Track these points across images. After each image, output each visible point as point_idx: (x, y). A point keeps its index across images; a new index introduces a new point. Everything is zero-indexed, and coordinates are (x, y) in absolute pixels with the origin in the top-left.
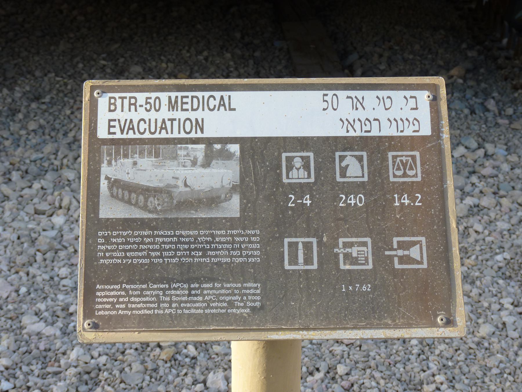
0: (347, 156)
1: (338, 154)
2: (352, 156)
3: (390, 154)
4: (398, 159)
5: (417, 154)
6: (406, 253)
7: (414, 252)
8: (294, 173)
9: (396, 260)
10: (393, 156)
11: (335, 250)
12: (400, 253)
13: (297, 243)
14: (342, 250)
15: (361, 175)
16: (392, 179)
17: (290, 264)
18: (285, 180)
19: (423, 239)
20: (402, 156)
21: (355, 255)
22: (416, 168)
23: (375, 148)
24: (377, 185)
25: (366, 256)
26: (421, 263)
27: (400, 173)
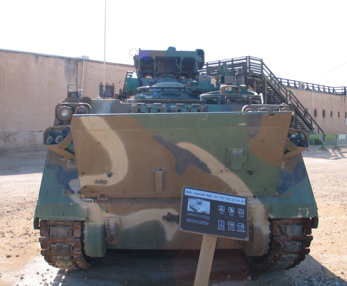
7: (242, 226)
12: (239, 226)
23: (236, 207)
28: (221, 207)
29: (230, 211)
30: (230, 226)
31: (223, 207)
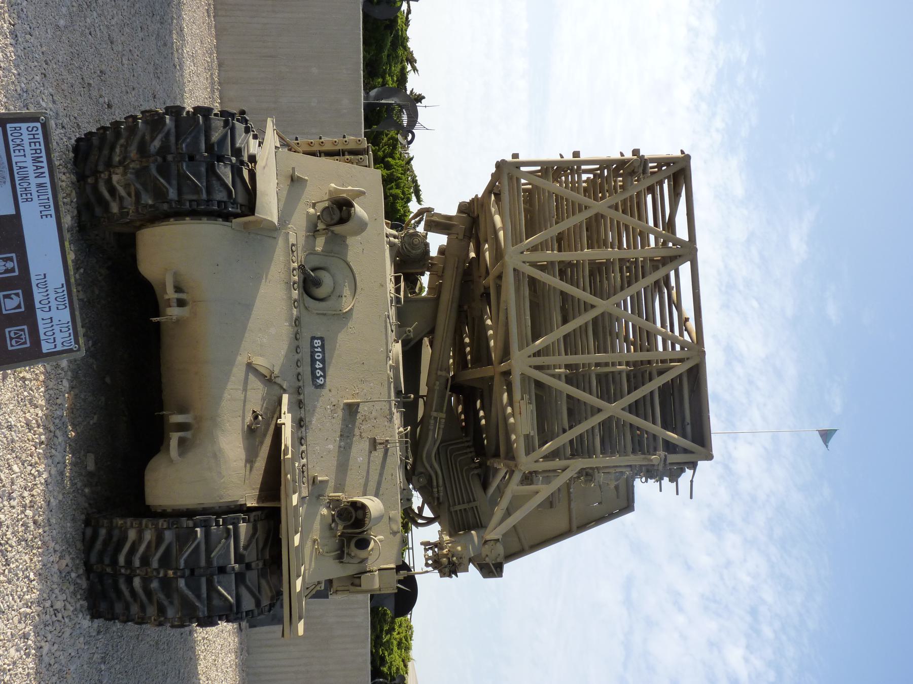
1: (20, 291)
3: (25, 327)
5: (28, 345)
16: (7, 330)
27: (12, 335)
31: (13, 270)
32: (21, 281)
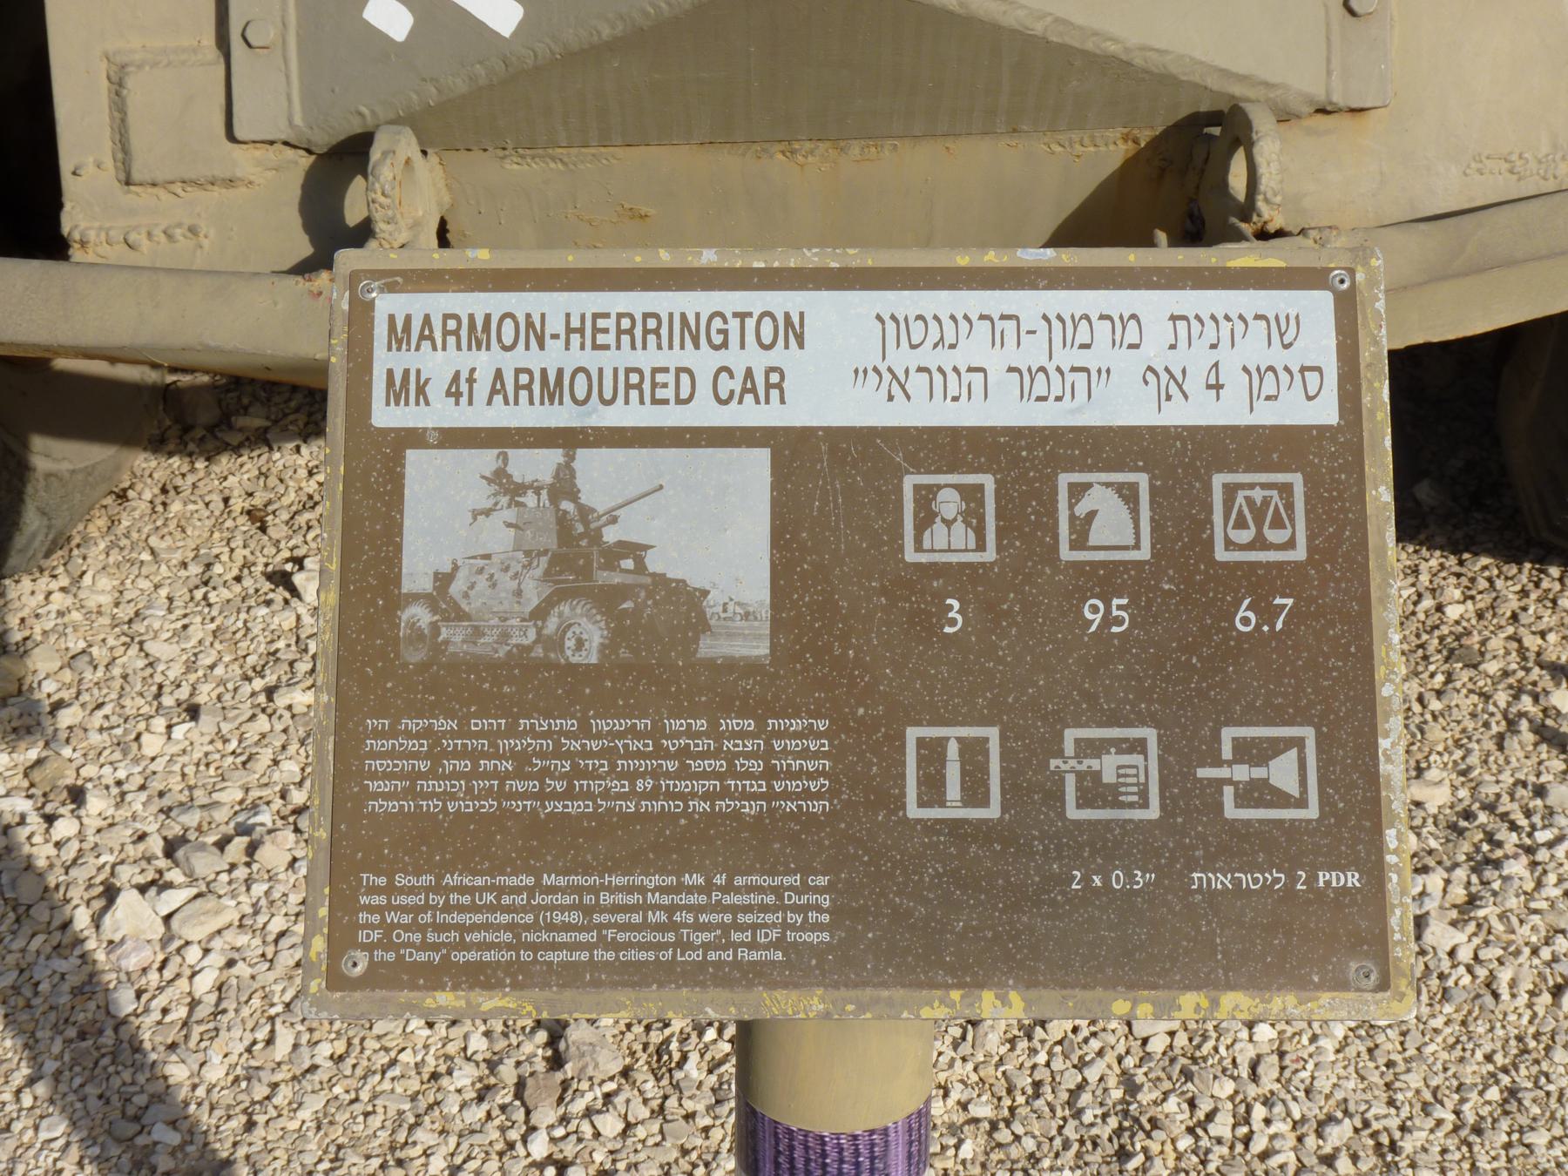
0: (1089, 486)
1: (1064, 480)
2: (1107, 485)
3: (1219, 480)
4: (1241, 495)
5: (1296, 480)
6: (1259, 773)
7: (1282, 773)
8: (937, 535)
9: (1228, 791)
10: (1225, 486)
11: (1054, 763)
13: (942, 742)
14: (1072, 763)
15: (1132, 542)
16: (1221, 555)
17: (921, 804)
18: (911, 556)
19: (1308, 733)
20: (1251, 486)
21: (1109, 777)
22: (1293, 527)
24: (1182, 571)
25: (1142, 779)
26: (1302, 803)
28: (933, 490)
29: (1082, 527)
30: (1094, 791)
31: (972, 495)
32: (1025, 465)
